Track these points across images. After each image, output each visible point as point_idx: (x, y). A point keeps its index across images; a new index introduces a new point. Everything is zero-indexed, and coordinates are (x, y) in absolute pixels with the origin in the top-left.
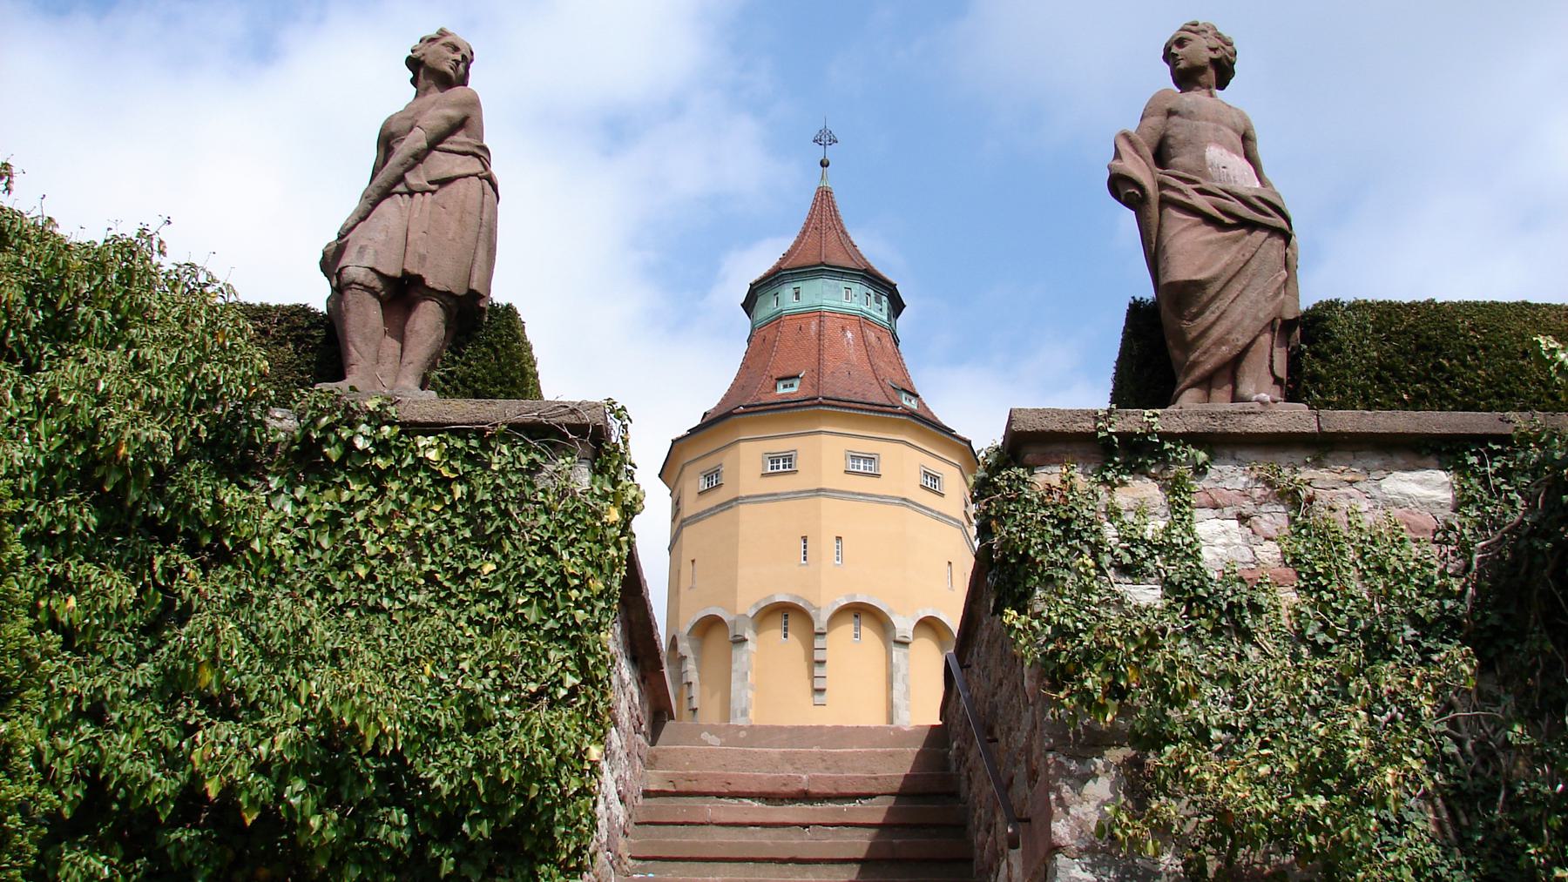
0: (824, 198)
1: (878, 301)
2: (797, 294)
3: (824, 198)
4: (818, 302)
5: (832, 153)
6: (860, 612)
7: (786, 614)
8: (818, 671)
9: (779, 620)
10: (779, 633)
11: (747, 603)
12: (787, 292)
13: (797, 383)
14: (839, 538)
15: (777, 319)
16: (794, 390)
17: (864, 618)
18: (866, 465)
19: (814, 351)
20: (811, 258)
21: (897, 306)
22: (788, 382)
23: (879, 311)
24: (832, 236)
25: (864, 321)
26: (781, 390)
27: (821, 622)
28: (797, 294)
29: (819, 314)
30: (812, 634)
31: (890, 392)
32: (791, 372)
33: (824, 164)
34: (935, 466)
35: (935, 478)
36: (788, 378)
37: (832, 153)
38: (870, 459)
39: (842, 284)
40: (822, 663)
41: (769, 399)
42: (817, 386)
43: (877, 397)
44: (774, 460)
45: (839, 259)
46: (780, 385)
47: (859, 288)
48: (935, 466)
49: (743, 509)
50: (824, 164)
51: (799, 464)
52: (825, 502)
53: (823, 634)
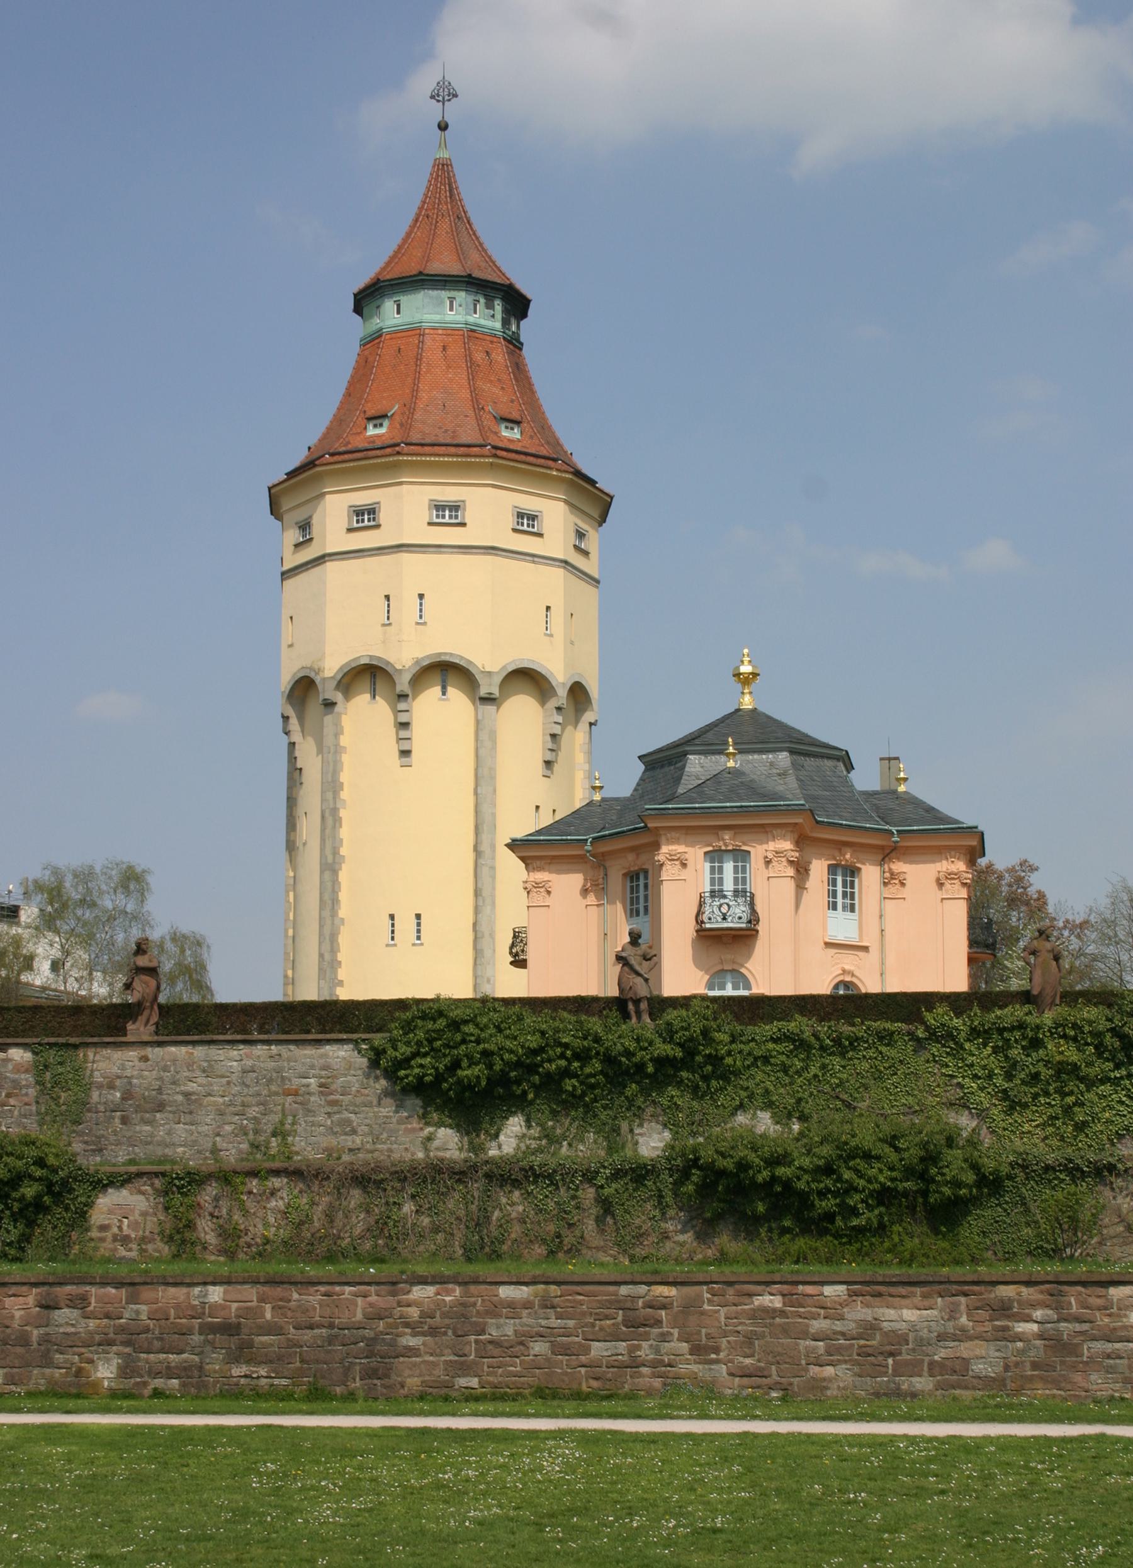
0: (443, 173)
1: (490, 306)
2: (399, 306)
3: (443, 173)
4: (417, 317)
5: (453, 112)
6: (445, 671)
7: (369, 675)
8: (403, 734)
9: (366, 682)
10: (367, 697)
11: (332, 665)
12: (389, 305)
13: (386, 423)
17: (451, 678)
18: (448, 513)
20: (410, 267)
21: (517, 305)
22: (378, 422)
23: (488, 318)
25: (472, 333)
27: (403, 684)
28: (399, 306)
29: (417, 332)
31: (488, 422)
34: (530, 503)
35: (532, 518)
36: (377, 418)
37: (453, 112)
38: (455, 508)
39: (445, 294)
40: (405, 725)
41: (358, 443)
42: (406, 426)
43: (469, 435)
44: (359, 512)
45: (444, 263)
46: (370, 427)
47: (461, 296)
48: (530, 503)
49: (330, 566)
50: (443, 127)
51: (383, 517)
52: (405, 557)
53: (407, 696)
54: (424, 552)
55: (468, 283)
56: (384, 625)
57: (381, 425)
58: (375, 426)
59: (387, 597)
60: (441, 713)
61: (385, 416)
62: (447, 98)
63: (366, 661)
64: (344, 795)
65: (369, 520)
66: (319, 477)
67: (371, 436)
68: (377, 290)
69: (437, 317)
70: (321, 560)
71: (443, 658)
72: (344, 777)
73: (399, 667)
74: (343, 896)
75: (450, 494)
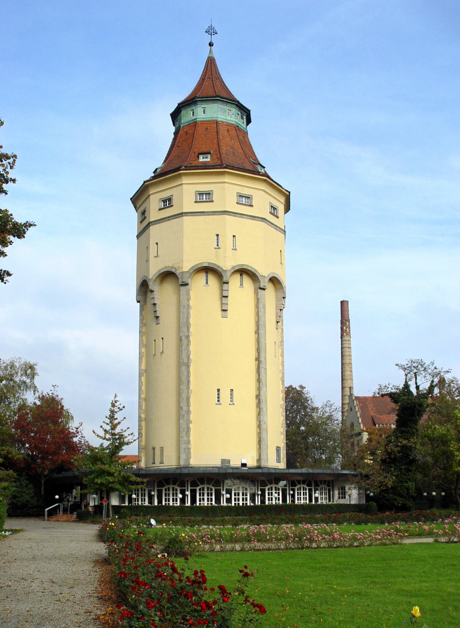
0: (211, 64)
1: (242, 118)
3: (211, 64)
4: (215, 115)
5: (215, 39)
13: (209, 156)
14: (234, 236)
15: (195, 124)
16: (209, 160)
19: (215, 141)
21: (249, 121)
22: (205, 156)
23: (242, 123)
24: (218, 83)
25: (237, 128)
26: (201, 159)
30: (223, 282)
32: (204, 150)
33: (211, 45)
35: (275, 209)
37: (215, 39)
38: (248, 198)
41: (195, 163)
46: (201, 157)
47: (234, 110)
49: (185, 219)
50: (211, 45)
54: (235, 216)
55: (237, 105)
56: (215, 248)
57: (207, 158)
58: (203, 158)
59: (217, 235)
60: (241, 293)
61: (209, 153)
62: (212, 33)
63: (207, 265)
64: (191, 329)
65: (206, 199)
66: (180, 176)
67: (202, 162)
68: (193, 102)
69: (224, 117)
70: (181, 215)
71: (244, 267)
72: (191, 321)
73: (224, 269)
74: (191, 379)
75: (246, 192)
